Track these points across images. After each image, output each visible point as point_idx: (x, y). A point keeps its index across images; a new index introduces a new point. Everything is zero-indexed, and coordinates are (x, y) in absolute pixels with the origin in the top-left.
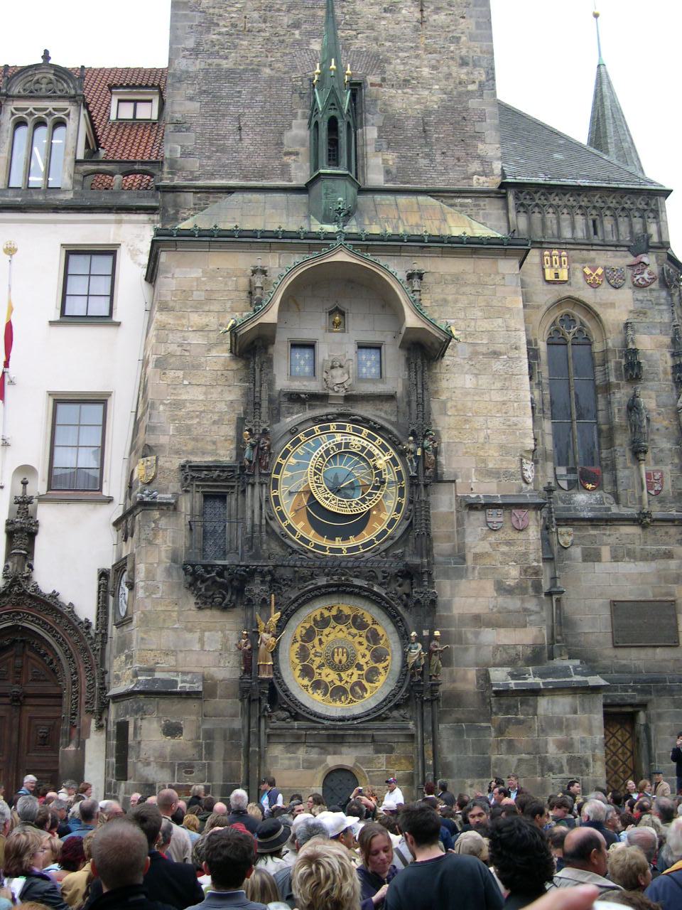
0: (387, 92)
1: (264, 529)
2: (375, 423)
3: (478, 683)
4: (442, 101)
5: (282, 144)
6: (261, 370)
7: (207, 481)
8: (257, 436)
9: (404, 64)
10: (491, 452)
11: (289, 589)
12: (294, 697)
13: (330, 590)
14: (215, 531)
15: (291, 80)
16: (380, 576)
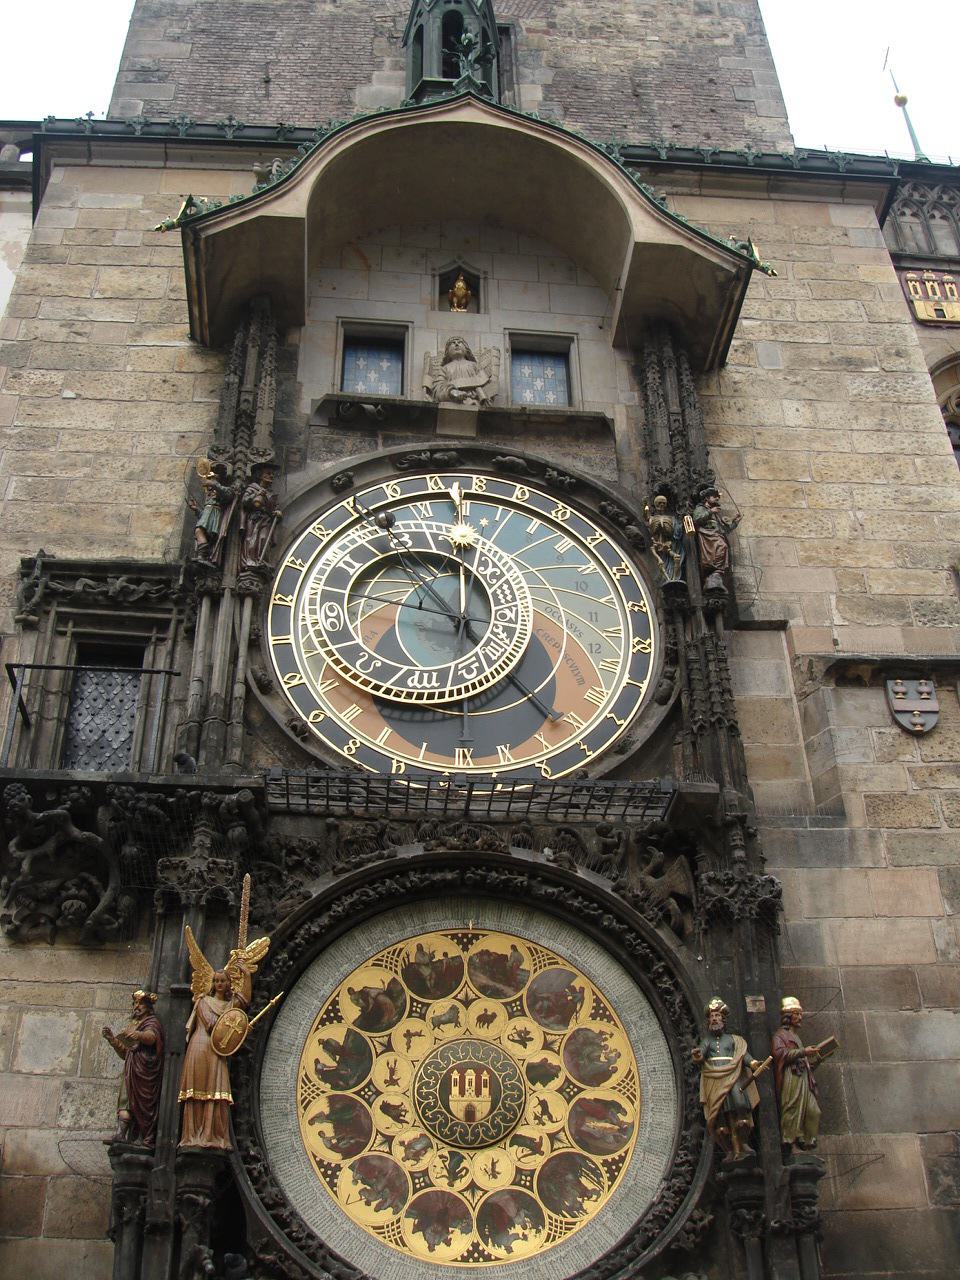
0: (561, 42)
1: (237, 710)
2: (562, 473)
3: (934, 1182)
4: (666, 56)
5: (350, 102)
6: (261, 355)
7: (96, 605)
8: (238, 483)
9: (589, 7)
10: (873, 560)
11: (307, 881)
12: (302, 1225)
13: (438, 876)
14: (101, 744)
15: (372, 20)
16: (593, 844)
